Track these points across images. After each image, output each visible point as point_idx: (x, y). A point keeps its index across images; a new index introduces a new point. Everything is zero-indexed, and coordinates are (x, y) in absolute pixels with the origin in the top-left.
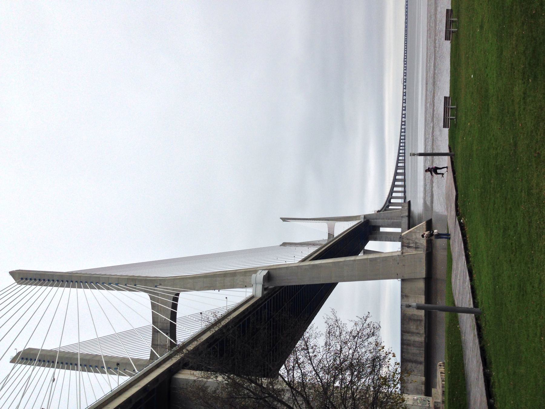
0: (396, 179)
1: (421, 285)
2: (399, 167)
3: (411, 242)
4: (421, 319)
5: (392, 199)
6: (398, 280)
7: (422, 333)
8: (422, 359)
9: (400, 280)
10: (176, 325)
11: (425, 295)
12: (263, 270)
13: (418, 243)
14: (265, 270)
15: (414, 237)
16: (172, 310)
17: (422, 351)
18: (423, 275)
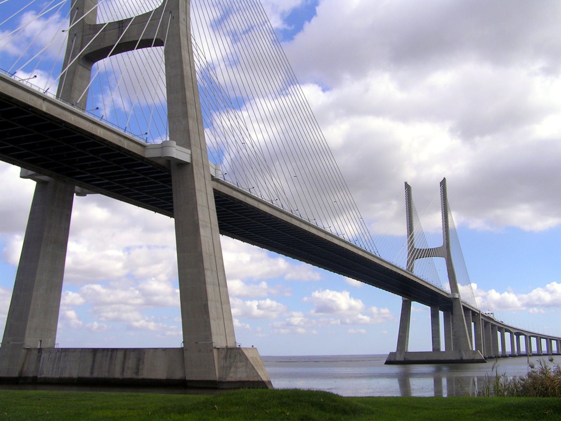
0: (541, 338)
1: (178, 375)
2: (551, 342)
3: (232, 360)
4: (139, 373)
5: (509, 333)
6: (182, 344)
7: (124, 374)
8: (95, 375)
9: (183, 346)
10: (134, 49)
11: (167, 380)
12: (191, 155)
13: (230, 370)
14: (191, 158)
15: (239, 364)
16: (153, 39)
17: (129, 374)
18: (190, 377)
